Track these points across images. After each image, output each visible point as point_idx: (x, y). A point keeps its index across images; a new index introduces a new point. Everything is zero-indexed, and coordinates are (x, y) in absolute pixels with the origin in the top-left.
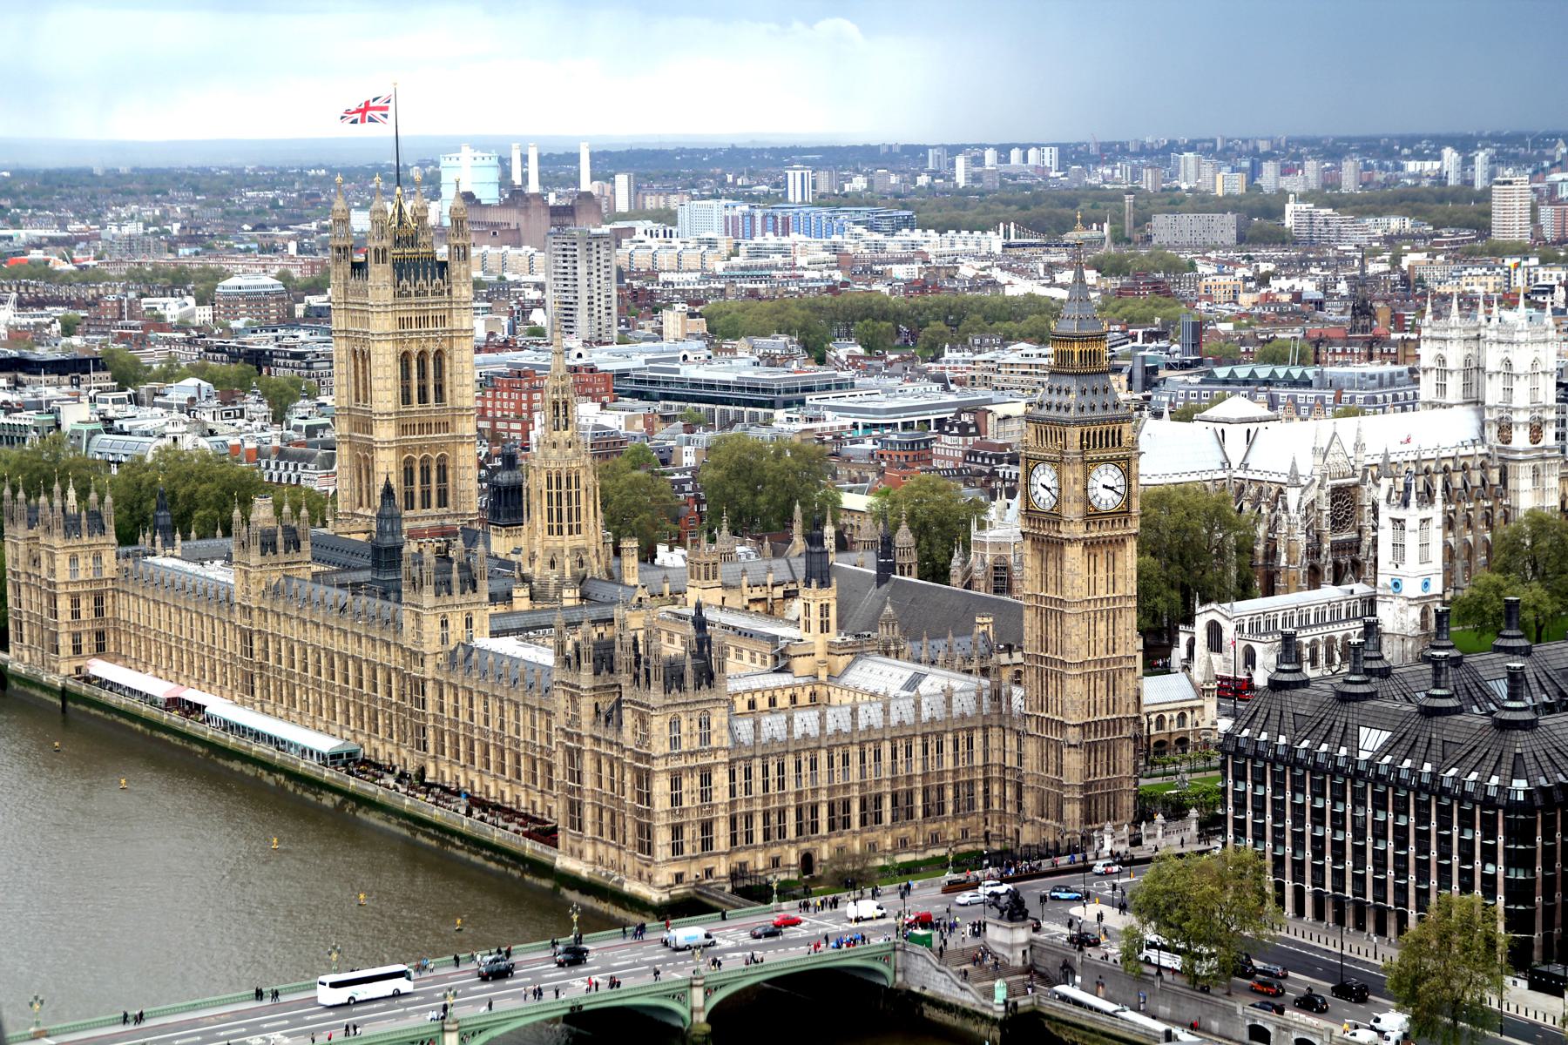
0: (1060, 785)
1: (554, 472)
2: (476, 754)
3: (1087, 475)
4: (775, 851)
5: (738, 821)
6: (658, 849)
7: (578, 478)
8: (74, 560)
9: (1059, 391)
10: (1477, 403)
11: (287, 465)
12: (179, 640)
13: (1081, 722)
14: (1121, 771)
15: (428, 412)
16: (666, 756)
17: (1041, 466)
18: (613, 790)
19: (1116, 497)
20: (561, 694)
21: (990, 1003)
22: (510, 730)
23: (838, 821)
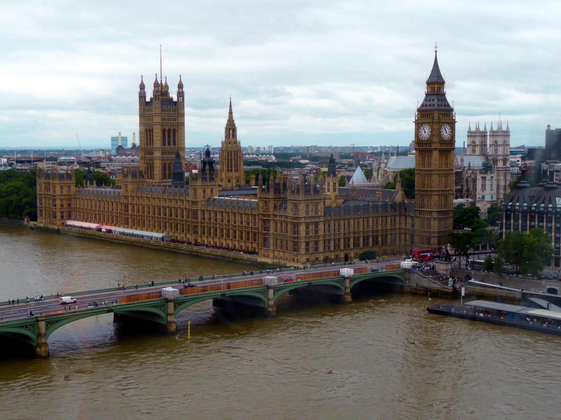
0: (430, 232)
1: (229, 152)
2: (218, 232)
3: (440, 128)
4: (337, 253)
5: (326, 242)
6: (302, 250)
7: (237, 154)
8: (62, 188)
9: (430, 100)
10: (484, 155)
11: (113, 177)
12: (99, 211)
13: (437, 210)
14: (448, 228)
15: (171, 148)
16: (305, 217)
17: (424, 125)
18: (282, 232)
19: (449, 135)
20: (261, 201)
21: (446, 287)
22: (232, 222)
23: (356, 245)
